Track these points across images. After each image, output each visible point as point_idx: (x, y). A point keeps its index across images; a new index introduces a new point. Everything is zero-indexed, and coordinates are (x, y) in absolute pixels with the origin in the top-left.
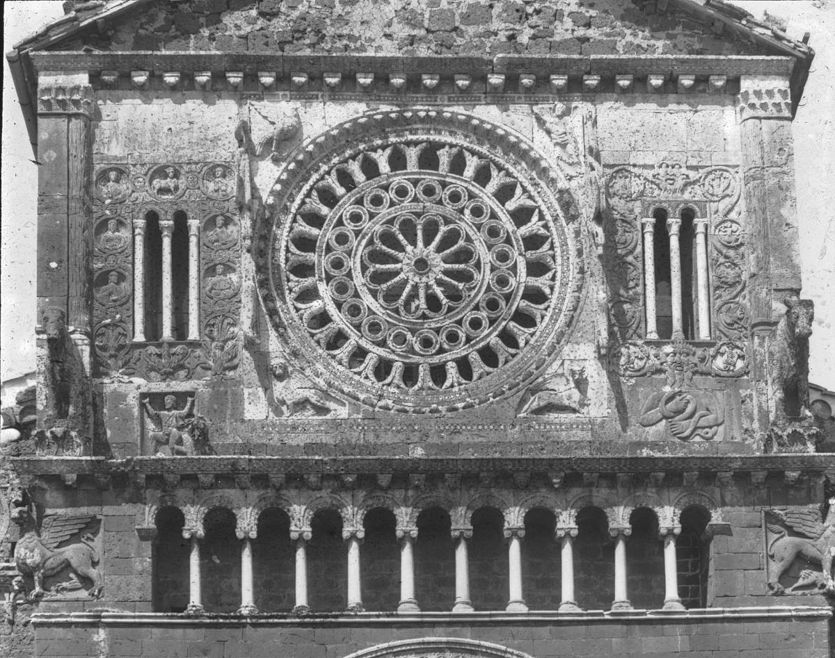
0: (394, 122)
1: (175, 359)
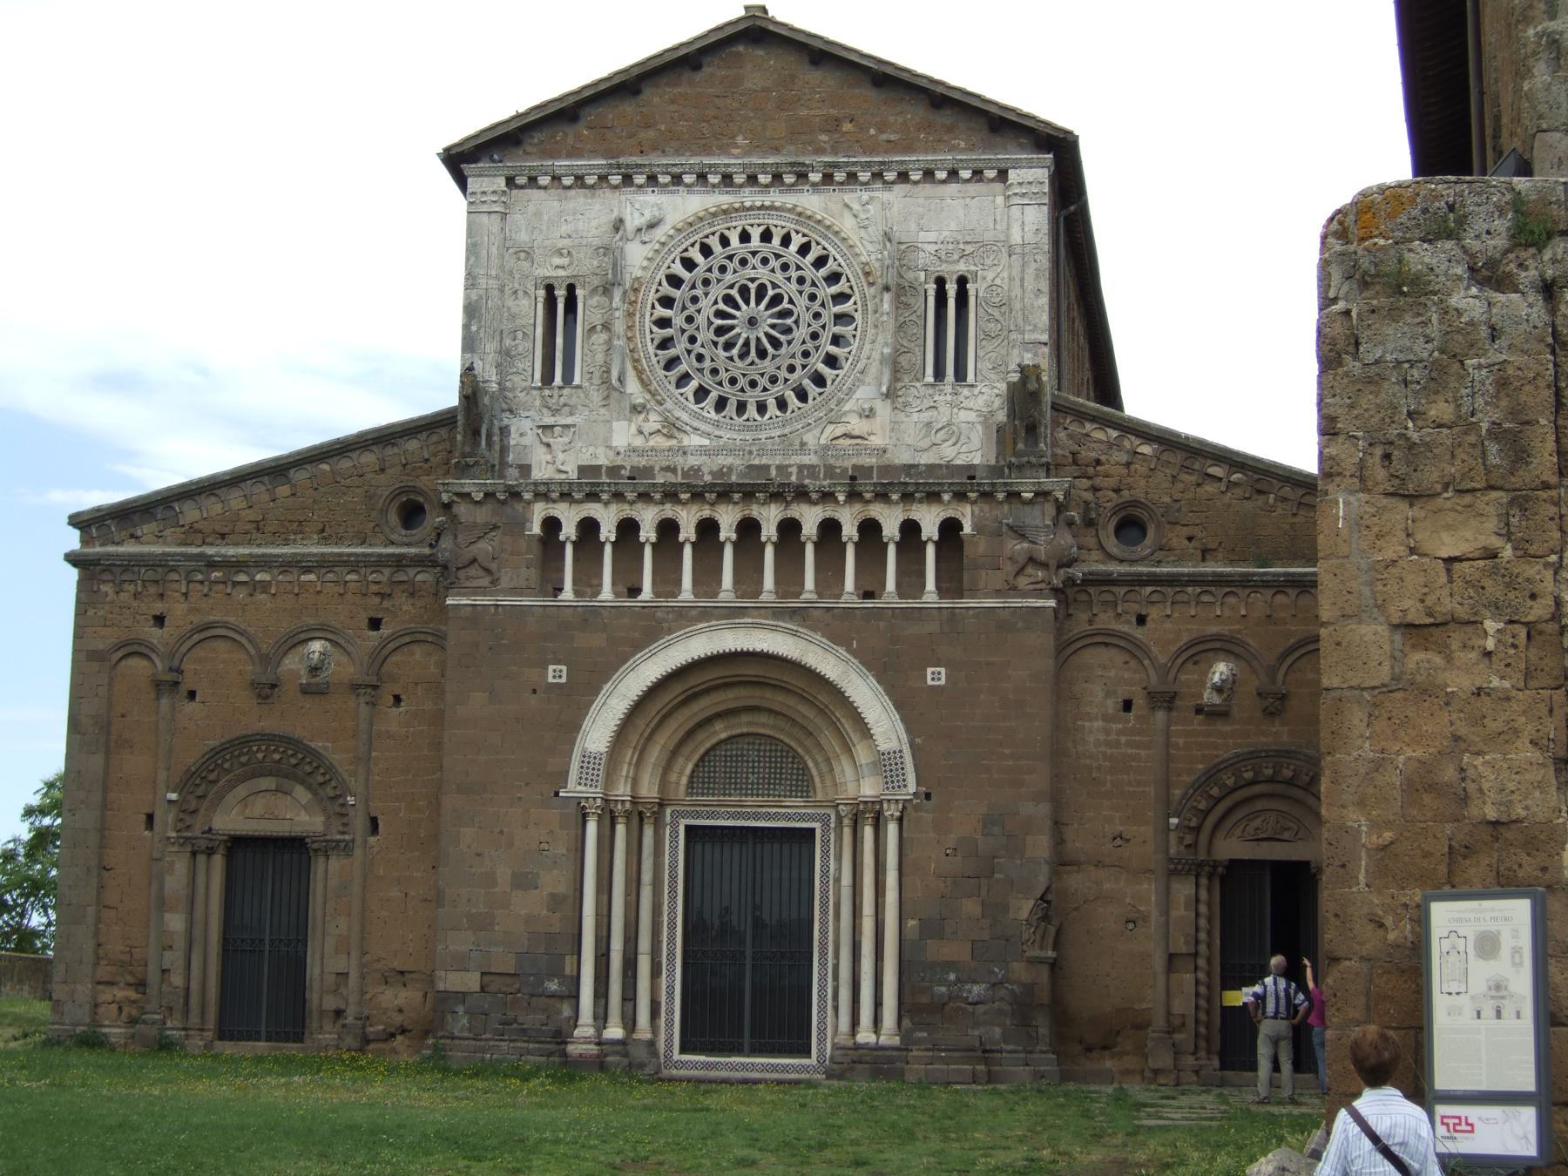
0: (736, 210)
1: (562, 400)
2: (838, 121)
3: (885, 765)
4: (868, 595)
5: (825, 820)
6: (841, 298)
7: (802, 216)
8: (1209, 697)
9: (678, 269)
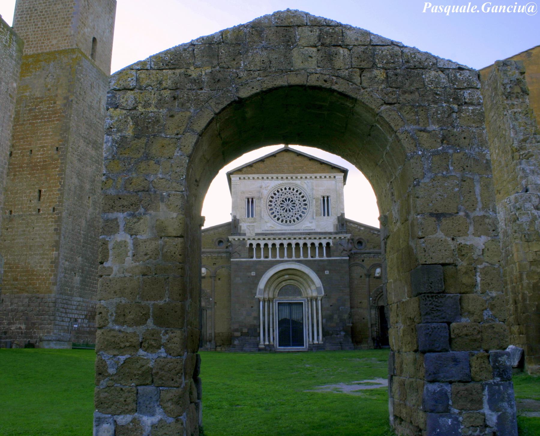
2: (303, 167)
3: (318, 289)
4: (312, 257)
5: (305, 300)
6: (304, 201)
7: (296, 185)
8: (377, 275)
9: (273, 195)
